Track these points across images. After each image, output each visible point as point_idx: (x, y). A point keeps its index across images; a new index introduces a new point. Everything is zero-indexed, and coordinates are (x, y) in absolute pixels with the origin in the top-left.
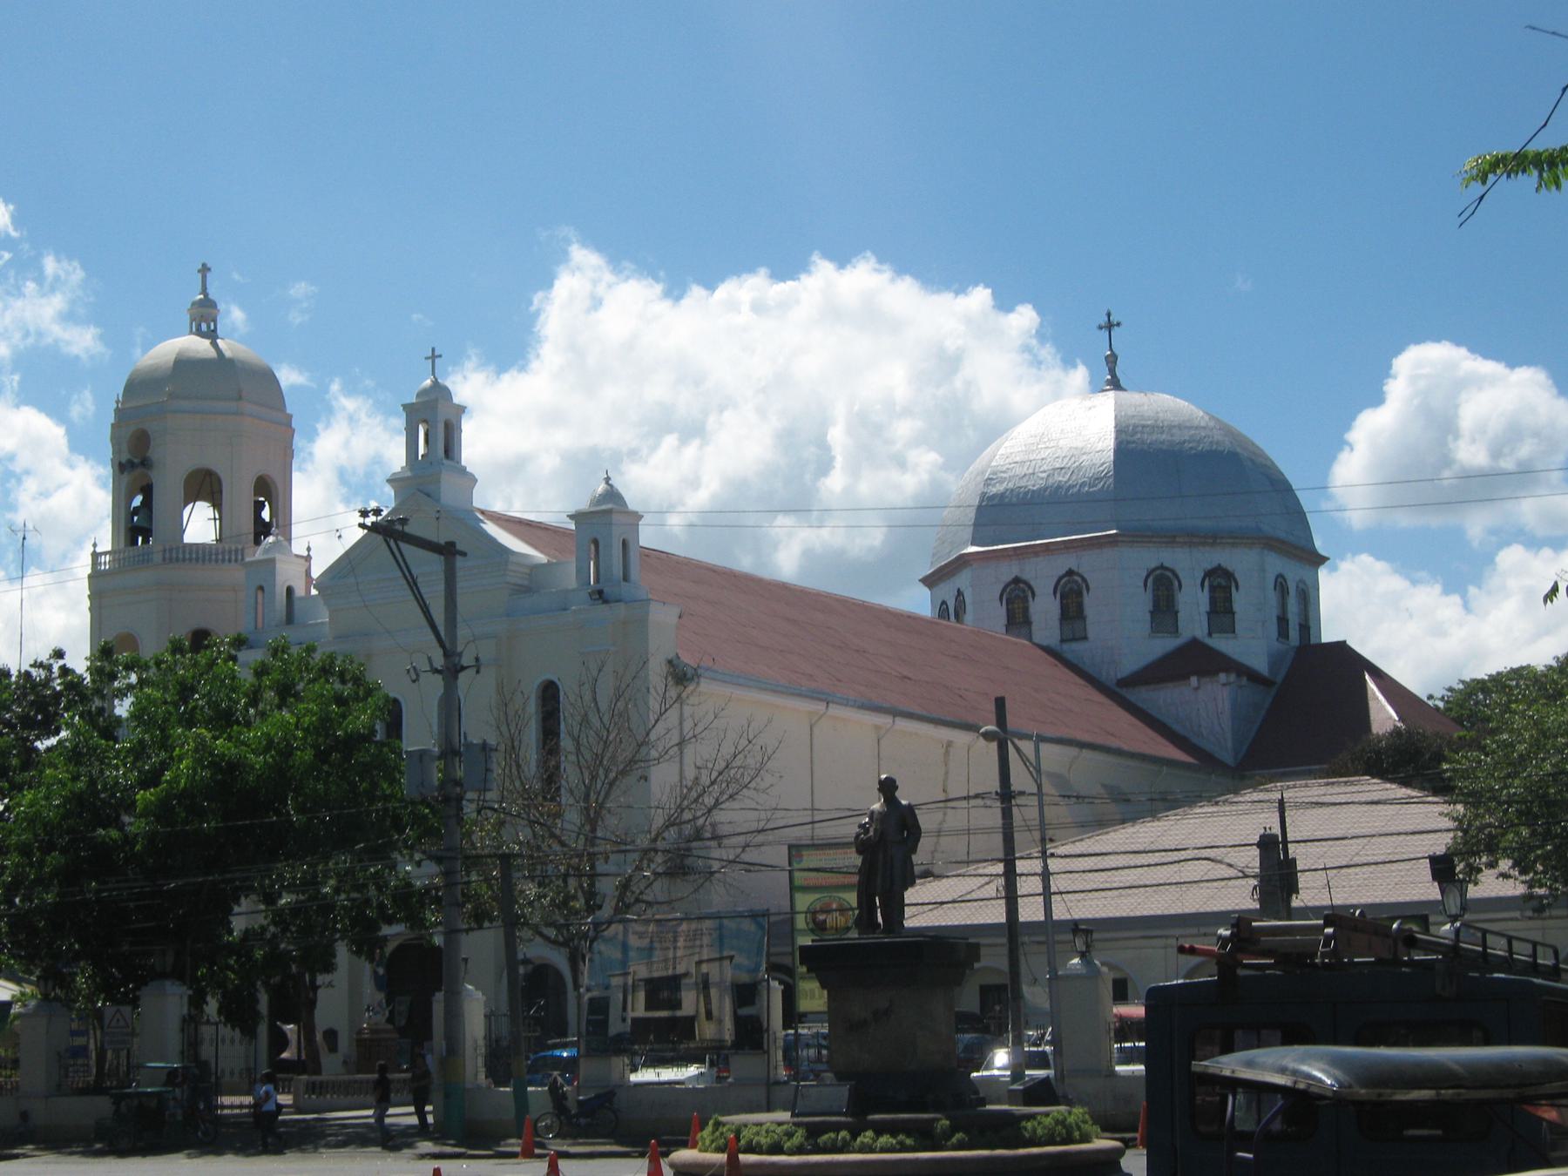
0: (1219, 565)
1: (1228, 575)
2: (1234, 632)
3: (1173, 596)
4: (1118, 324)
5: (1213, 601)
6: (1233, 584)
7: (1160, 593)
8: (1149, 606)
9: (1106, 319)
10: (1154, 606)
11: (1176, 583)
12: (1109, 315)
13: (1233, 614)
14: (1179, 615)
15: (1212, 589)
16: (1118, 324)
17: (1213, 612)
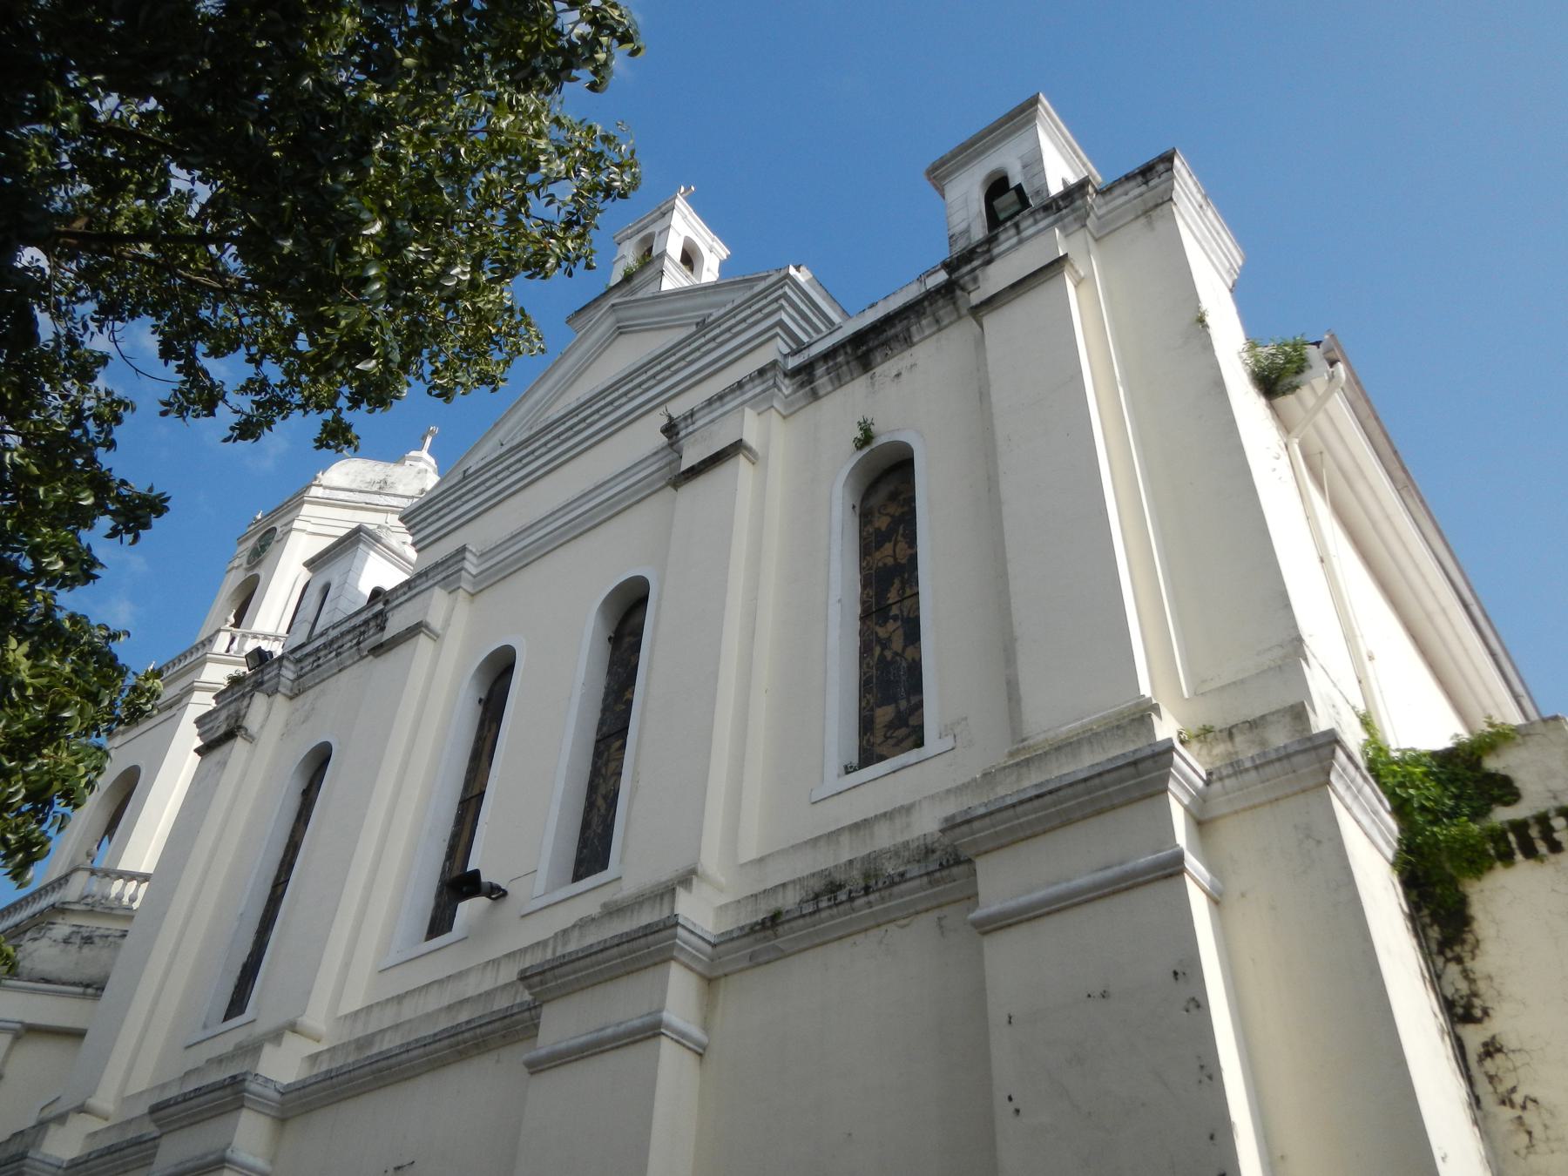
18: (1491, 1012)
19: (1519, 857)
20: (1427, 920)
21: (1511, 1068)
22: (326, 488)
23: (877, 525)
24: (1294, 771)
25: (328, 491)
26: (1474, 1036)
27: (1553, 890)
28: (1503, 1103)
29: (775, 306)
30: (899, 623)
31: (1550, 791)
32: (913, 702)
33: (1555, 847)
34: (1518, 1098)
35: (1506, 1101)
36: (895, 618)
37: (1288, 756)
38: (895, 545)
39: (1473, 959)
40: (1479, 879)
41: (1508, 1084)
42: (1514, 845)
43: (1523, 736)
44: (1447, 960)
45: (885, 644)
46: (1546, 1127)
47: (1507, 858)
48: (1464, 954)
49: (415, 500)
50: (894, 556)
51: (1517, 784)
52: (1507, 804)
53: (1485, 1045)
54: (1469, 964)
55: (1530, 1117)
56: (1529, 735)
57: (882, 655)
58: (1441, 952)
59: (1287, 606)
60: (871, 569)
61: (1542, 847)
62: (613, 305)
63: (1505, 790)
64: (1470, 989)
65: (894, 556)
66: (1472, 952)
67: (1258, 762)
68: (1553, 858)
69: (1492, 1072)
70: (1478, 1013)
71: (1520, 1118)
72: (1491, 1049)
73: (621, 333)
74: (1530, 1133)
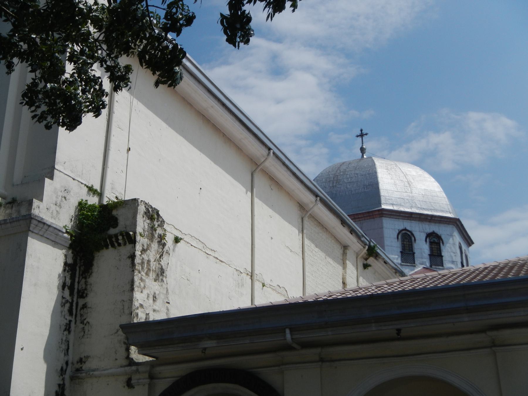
0: (434, 231)
1: (439, 237)
2: (443, 266)
3: (412, 245)
4: (366, 134)
5: (431, 249)
6: (441, 242)
7: (405, 243)
8: (399, 250)
9: (360, 132)
10: (402, 249)
11: (413, 239)
12: (361, 130)
13: (442, 256)
14: (415, 255)
15: (431, 243)
16: (366, 134)
17: (431, 255)
18: (88, 295)
19: (110, 246)
20: (82, 264)
21: (87, 313)
24: (20, 226)
26: (81, 302)
27: (115, 259)
28: (81, 323)
31: (125, 225)
33: (119, 245)
34: (85, 322)
35: (82, 322)
37: (19, 220)
39: (89, 278)
40: (99, 252)
41: (84, 318)
42: (109, 243)
43: (126, 204)
44: (83, 278)
46: (89, 331)
47: (107, 247)
48: (87, 276)
51: (119, 221)
52: (114, 228)
53: (83, 305)
54: (87, 280)
55: (86, 328)
56: (127, 204)
58: (82, 275)
59: (55, 153)
61: (116, 245)
63: (114, 222)
64: (85, 287)
66: (90, 276)
67: (11, 221)
68: (118, 248)
69: (82, 314)
70: (85, 295)
71: (84, 328)
72: (85, 306)
74: (84, 332)
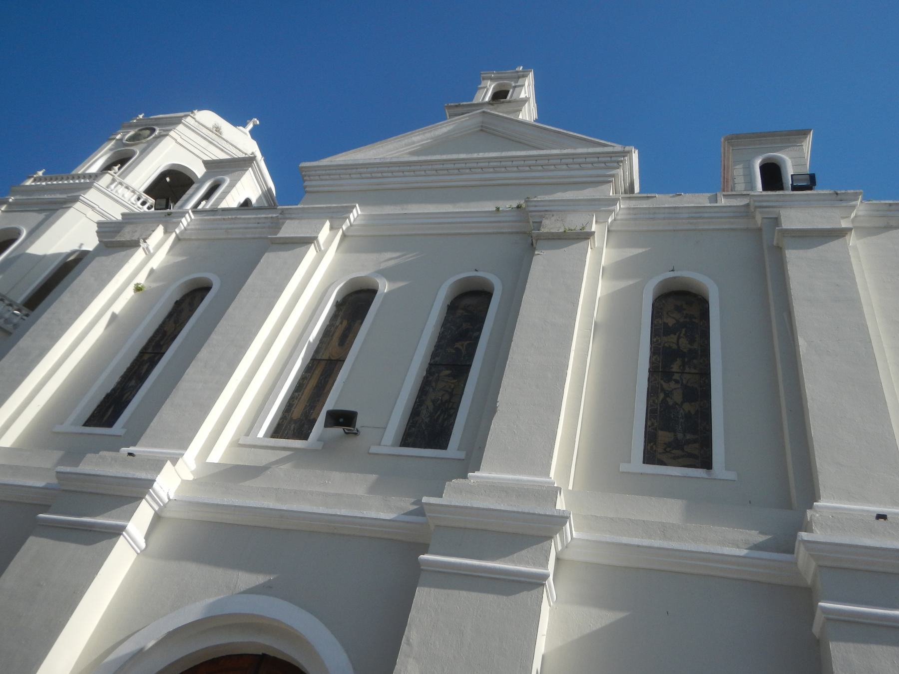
22: (196, 121)
23: (665, 320)
25: (197, 123)
29: (616, 164)
30: (679, 386)
32: (688, 438)
36: (677, 382)
38: (679, 338)
45: (668, 394)
49: (247, 156)
50: (678, 344)
57: (664, 401)
60: (660, 344)
62: (484, 112)
65: (678, 344)
73: (482, 130)
